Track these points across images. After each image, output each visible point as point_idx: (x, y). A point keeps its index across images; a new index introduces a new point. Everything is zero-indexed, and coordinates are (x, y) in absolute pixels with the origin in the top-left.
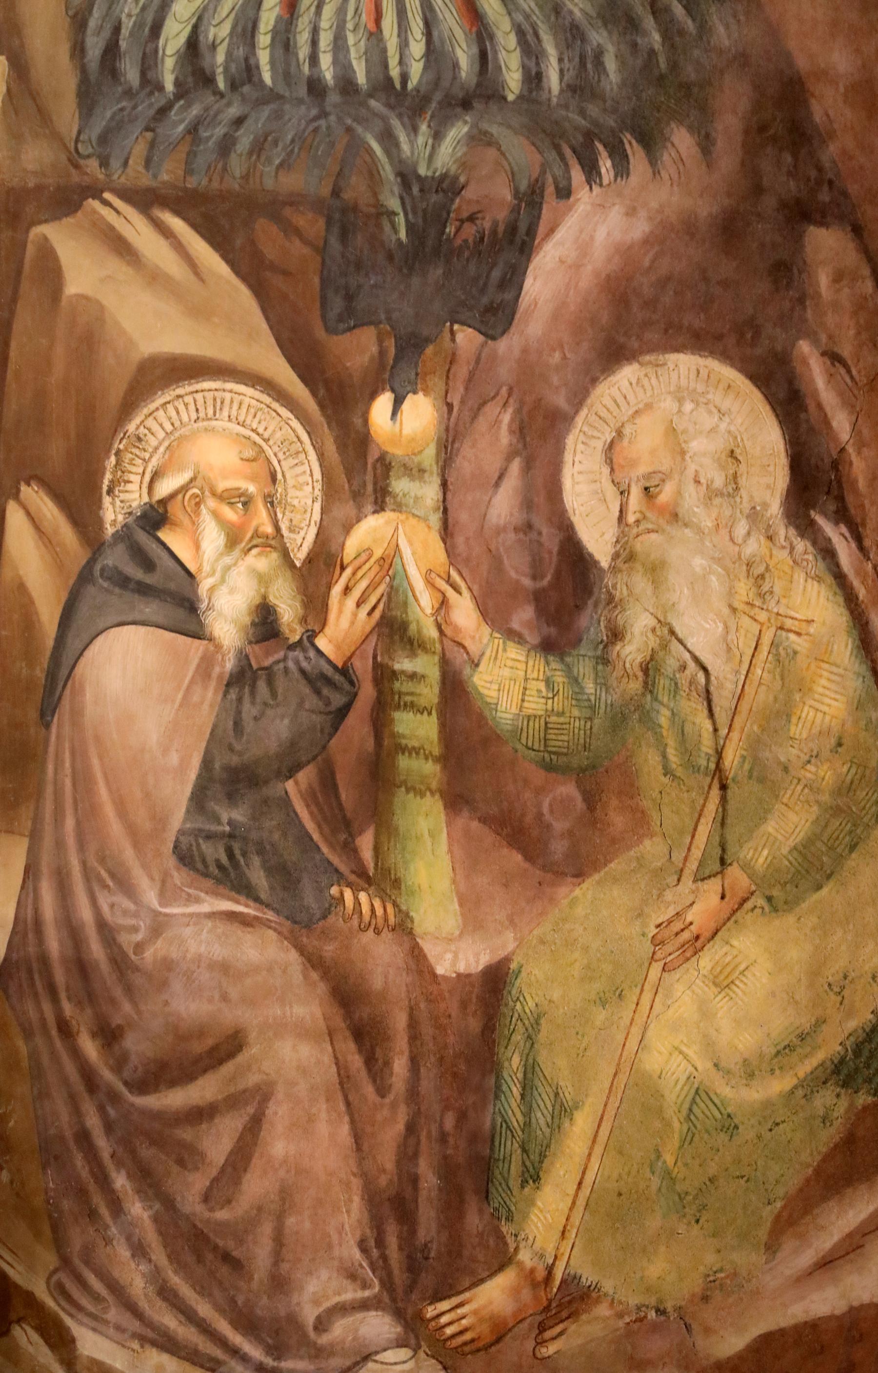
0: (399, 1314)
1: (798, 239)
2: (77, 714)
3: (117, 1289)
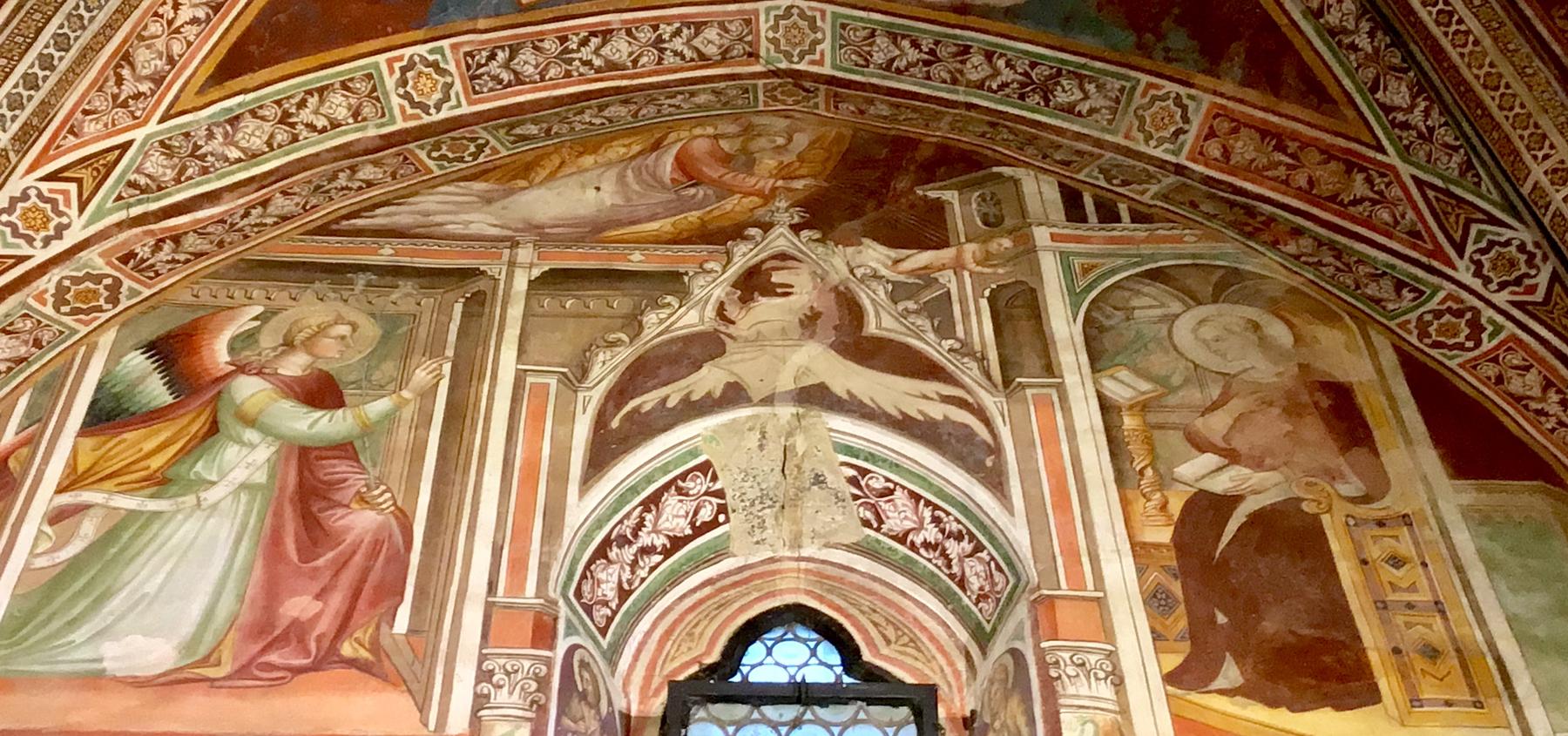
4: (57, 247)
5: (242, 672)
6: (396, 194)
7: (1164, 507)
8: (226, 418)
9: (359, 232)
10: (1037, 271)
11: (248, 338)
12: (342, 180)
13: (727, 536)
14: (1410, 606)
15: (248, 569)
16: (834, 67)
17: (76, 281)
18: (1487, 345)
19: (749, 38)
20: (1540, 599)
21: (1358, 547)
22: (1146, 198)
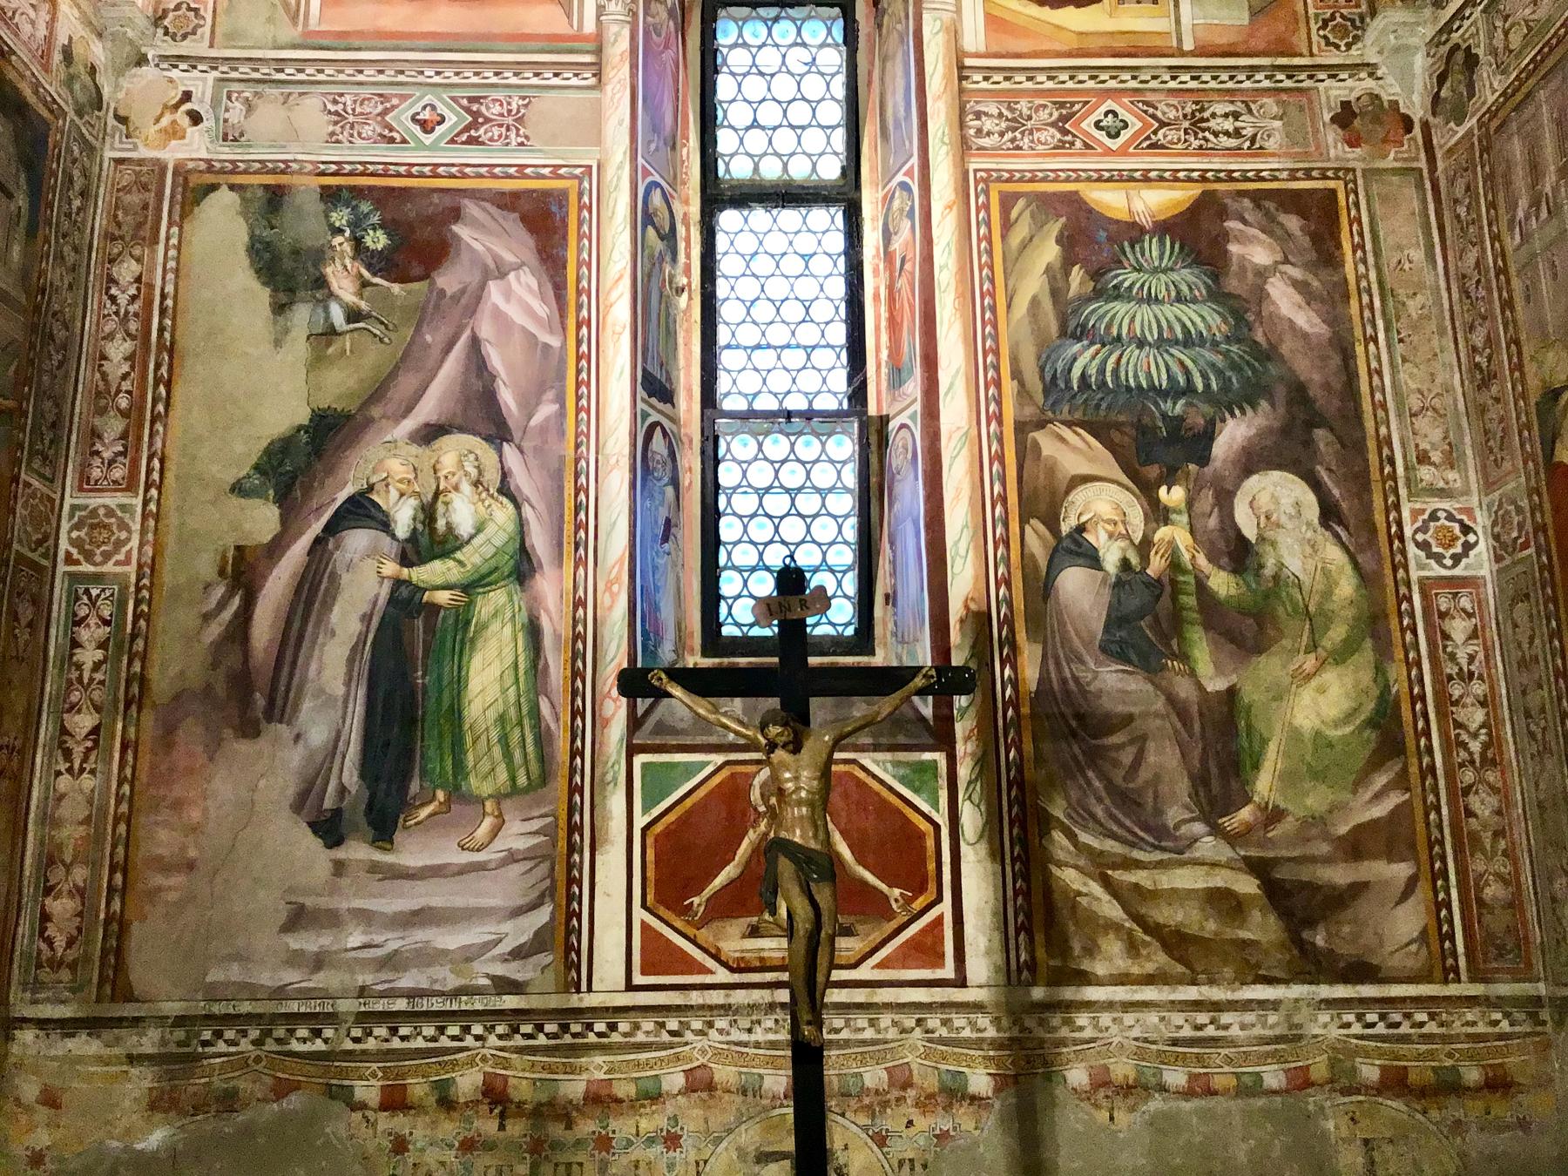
0: (1207, 822)
1: (1310, 433)
2: (1057, 598)
3: (1093, 816)
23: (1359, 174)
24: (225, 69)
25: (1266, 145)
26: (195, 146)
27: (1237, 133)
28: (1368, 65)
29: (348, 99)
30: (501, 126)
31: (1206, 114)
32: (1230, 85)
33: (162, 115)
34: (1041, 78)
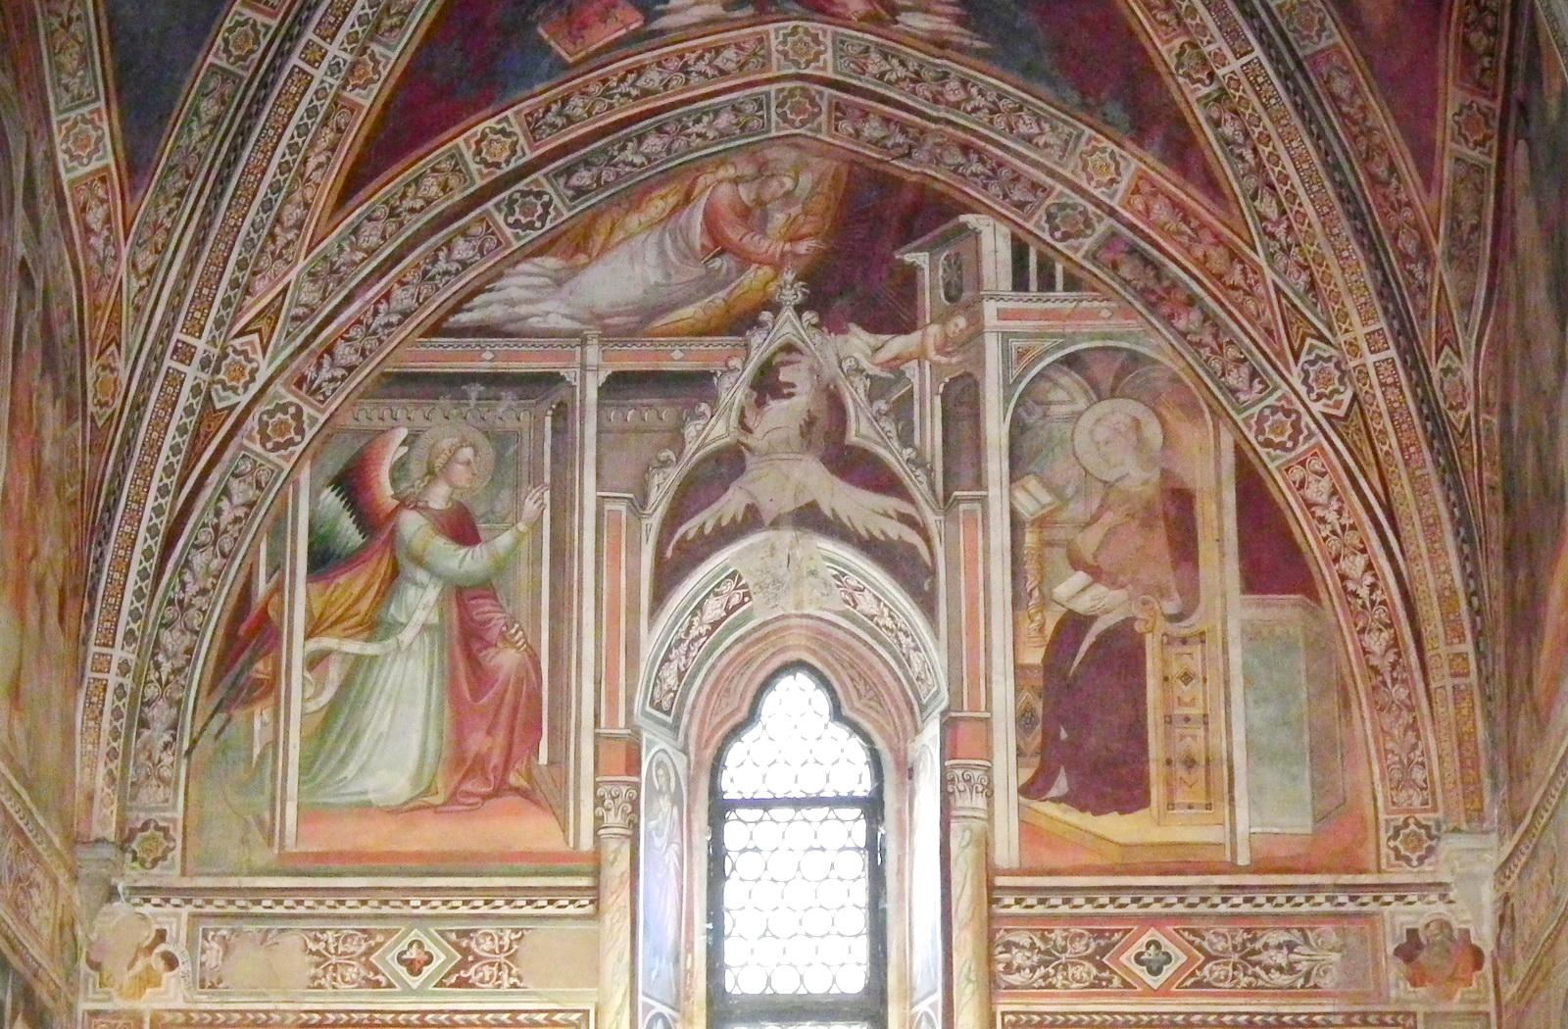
4: (254, 388)
5: (453, 798)
6: (485, 279)
7: (1041, 629)
8: (403, 561)
9: (462, 332)
10: (981, 362)
11: (400, 467)
12: (442, 265)
13: (751, 609)
14: (1187, 719)
15: (441, 712)
16: (836, 71)
17: (271, 414)
18: (1301, 448)
19: (762, 52)
20: (1271, 711)
21: (1165, 663)
22: (1078, 257)
23: (1420, 1017)
24: (199, 902)
25: (1321, 983)
26: (171, 995)
27: (1291, 969)
28: (1440, 884)
29: (330, 936)
30: (492, 964)
31: (1258, 945)
32: (1287, 908)
33: (135, 959)
34: (1079, 900)
